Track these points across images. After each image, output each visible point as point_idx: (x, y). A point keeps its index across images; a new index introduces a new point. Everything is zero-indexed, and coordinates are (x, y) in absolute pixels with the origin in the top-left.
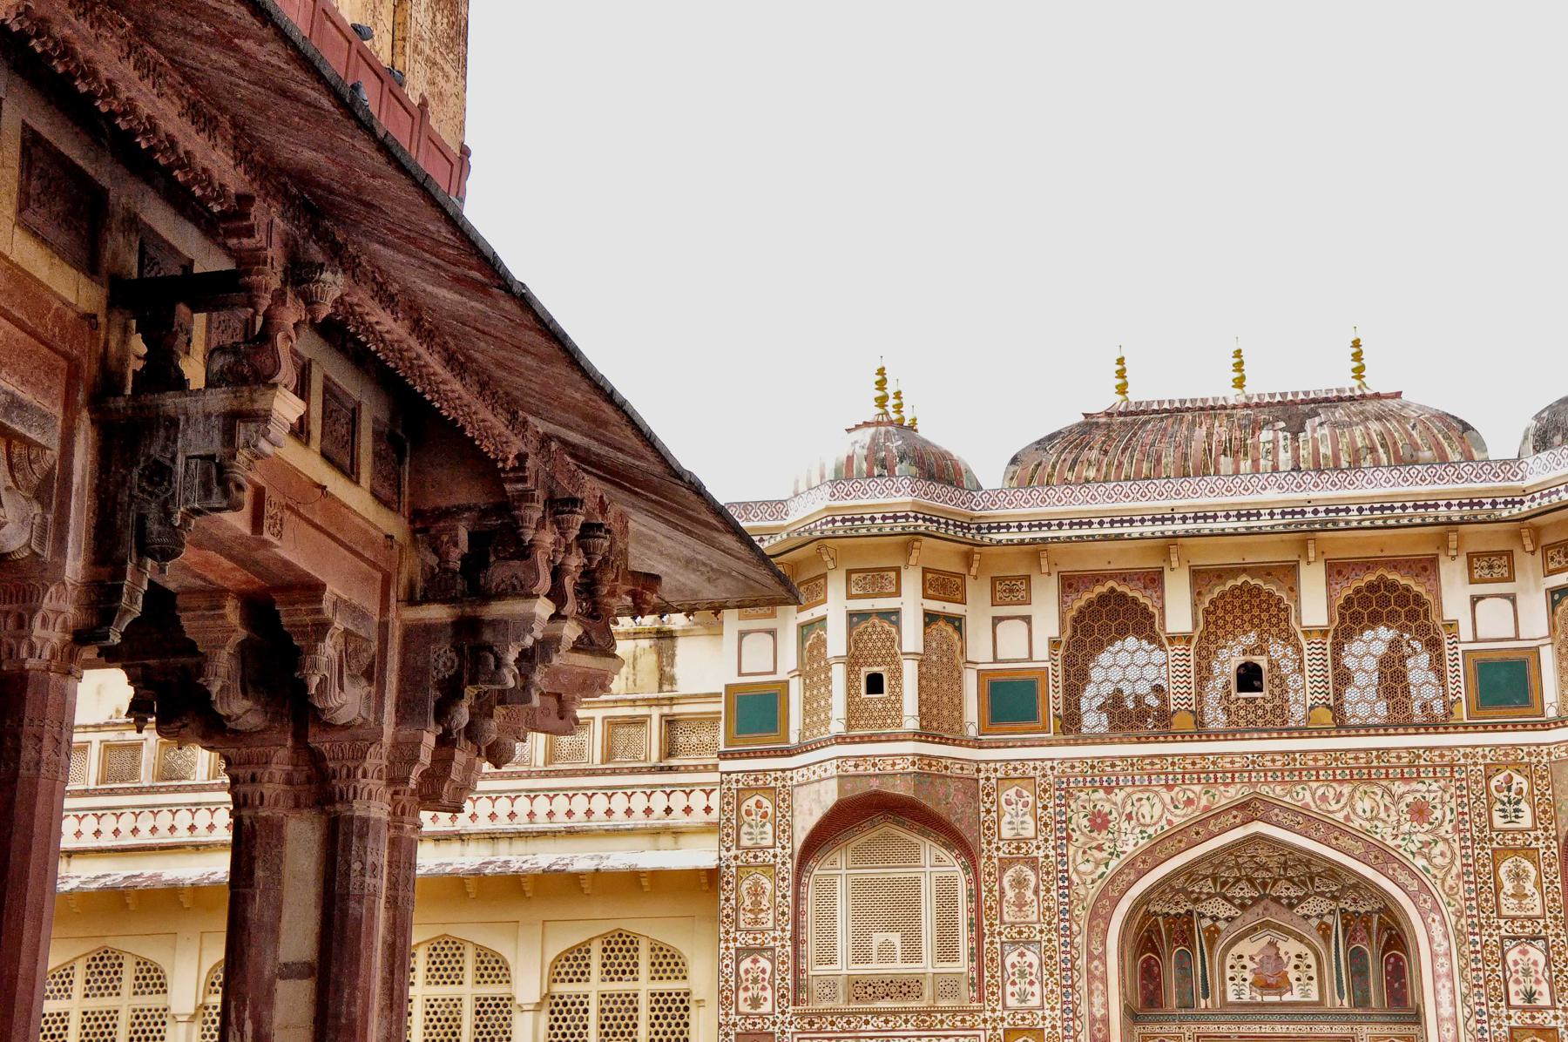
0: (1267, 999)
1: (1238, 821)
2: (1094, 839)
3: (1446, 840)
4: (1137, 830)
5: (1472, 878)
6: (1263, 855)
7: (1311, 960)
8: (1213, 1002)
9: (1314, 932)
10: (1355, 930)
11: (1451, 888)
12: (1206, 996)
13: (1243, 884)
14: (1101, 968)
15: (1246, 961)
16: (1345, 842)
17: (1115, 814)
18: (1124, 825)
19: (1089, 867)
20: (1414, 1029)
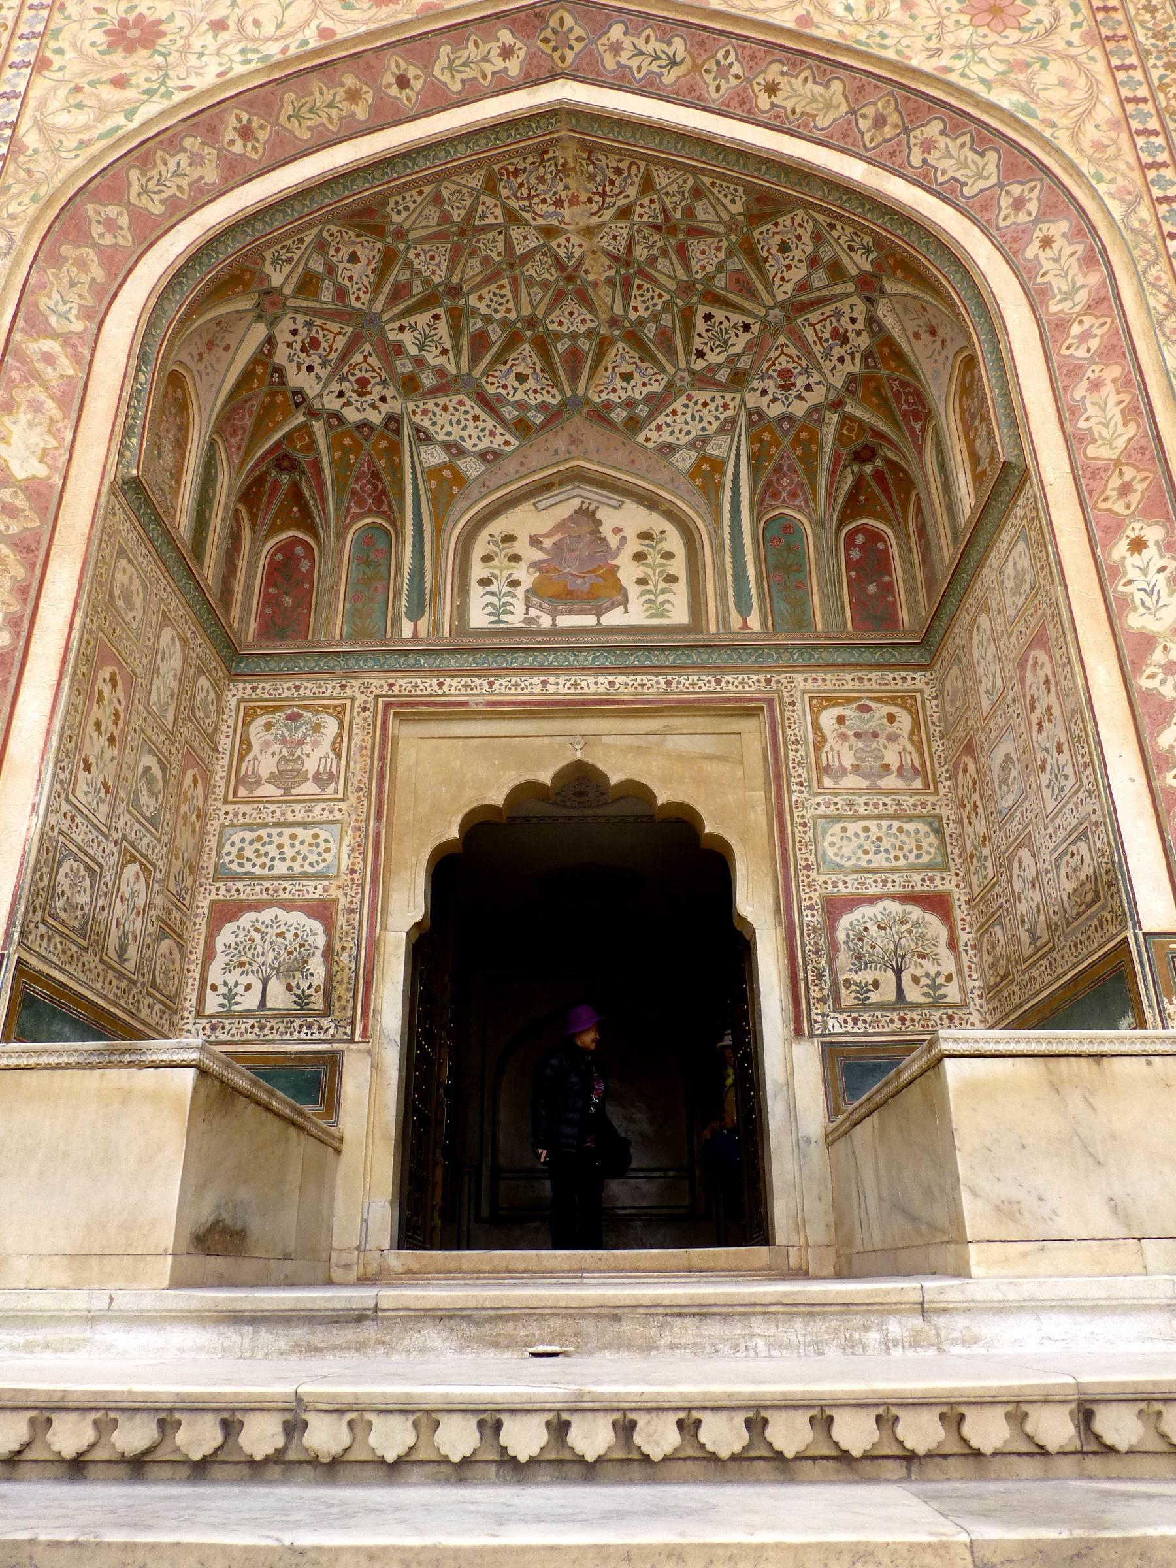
0: (564, 621)
1: (514, 67)
2: (114, 65)
3: (1073, 58)
4: (233, 50)
5: (1153, 124)
6: (579, 221)
7: (674, 542)
8: (434, 625)
9: (683, 483)
10: (778, 469)
11: (1099, 147)
12: (415, 613)
13: (525, 357)
14: (67, 367)
15: (522, 546)
16: (799, 92)
17: (180, 20)
18: (203, 39)
19: (81, 118)
20: (920, 680)
